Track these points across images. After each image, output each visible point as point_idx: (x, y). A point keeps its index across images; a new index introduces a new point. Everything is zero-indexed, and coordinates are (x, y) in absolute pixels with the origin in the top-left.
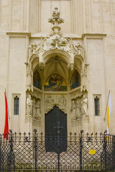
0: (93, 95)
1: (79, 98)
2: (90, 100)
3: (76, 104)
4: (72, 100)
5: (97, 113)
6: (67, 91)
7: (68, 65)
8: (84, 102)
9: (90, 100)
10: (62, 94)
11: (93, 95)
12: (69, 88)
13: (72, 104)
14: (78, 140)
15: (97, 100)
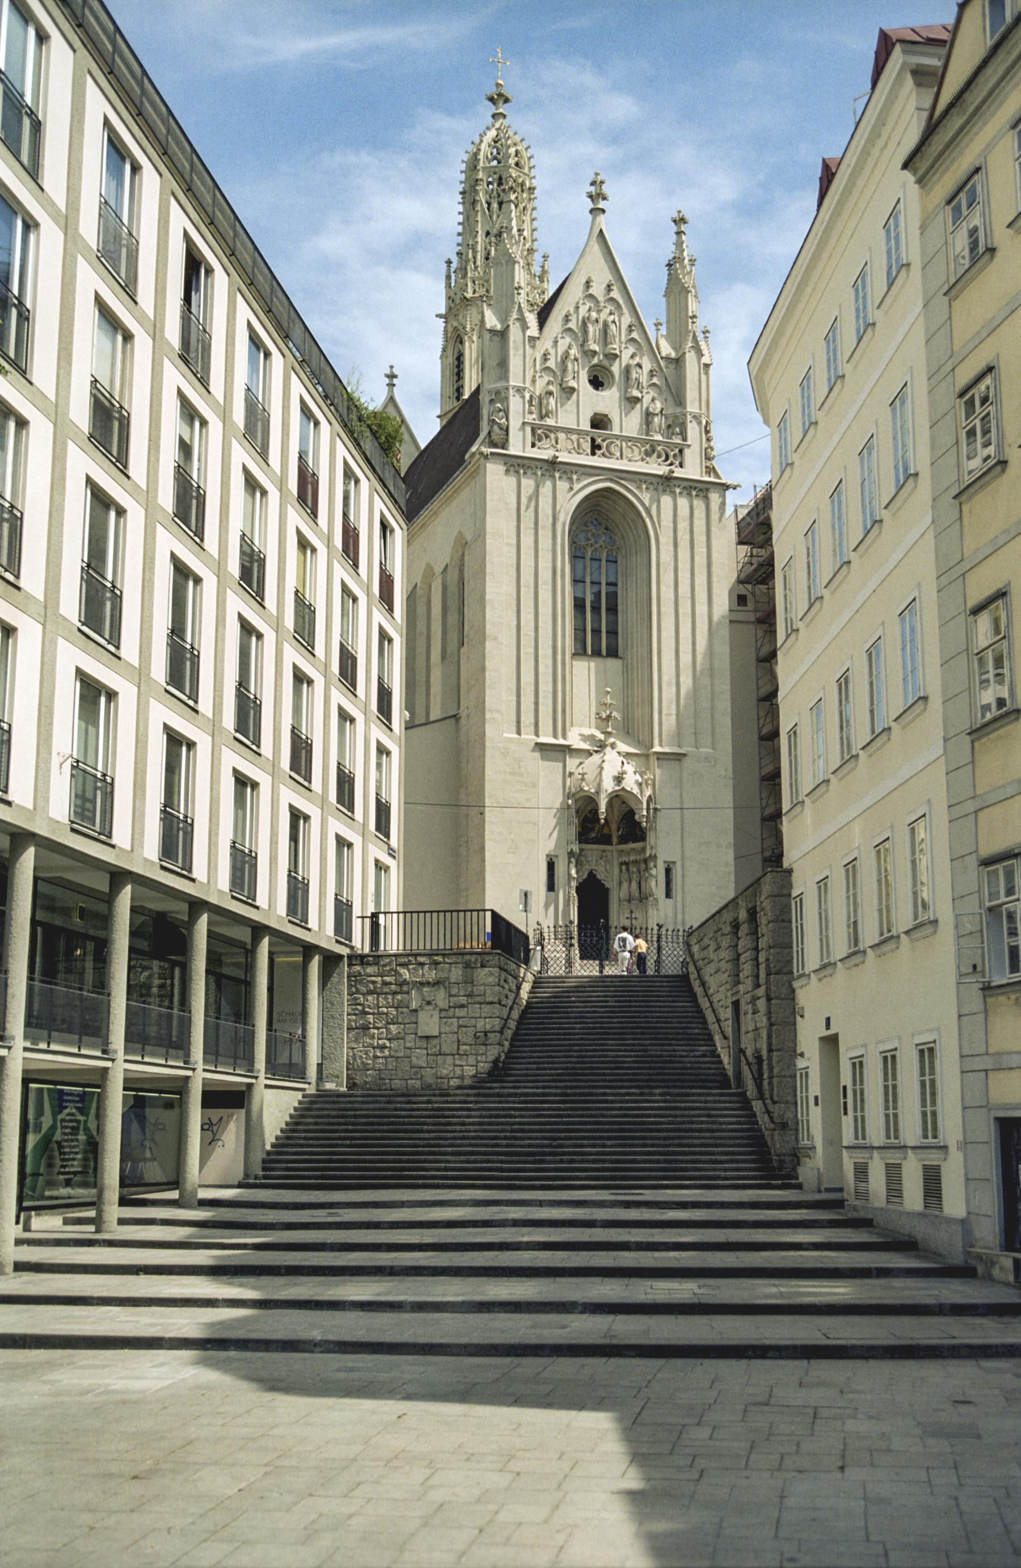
0: (665, 862)
1: (636, 862)
2: (658, 871)
3: (628, 870)
4: (621, 864)
5: (668, 894)
6: (611, 844)
7: (637, 817)
8: (651, 875)
9: (658, 871)
10: (604, 851)
11: (665, 862)
12: (615, 840)
13: (621, 871)
14: (655, 939)
15: (668, 871)
